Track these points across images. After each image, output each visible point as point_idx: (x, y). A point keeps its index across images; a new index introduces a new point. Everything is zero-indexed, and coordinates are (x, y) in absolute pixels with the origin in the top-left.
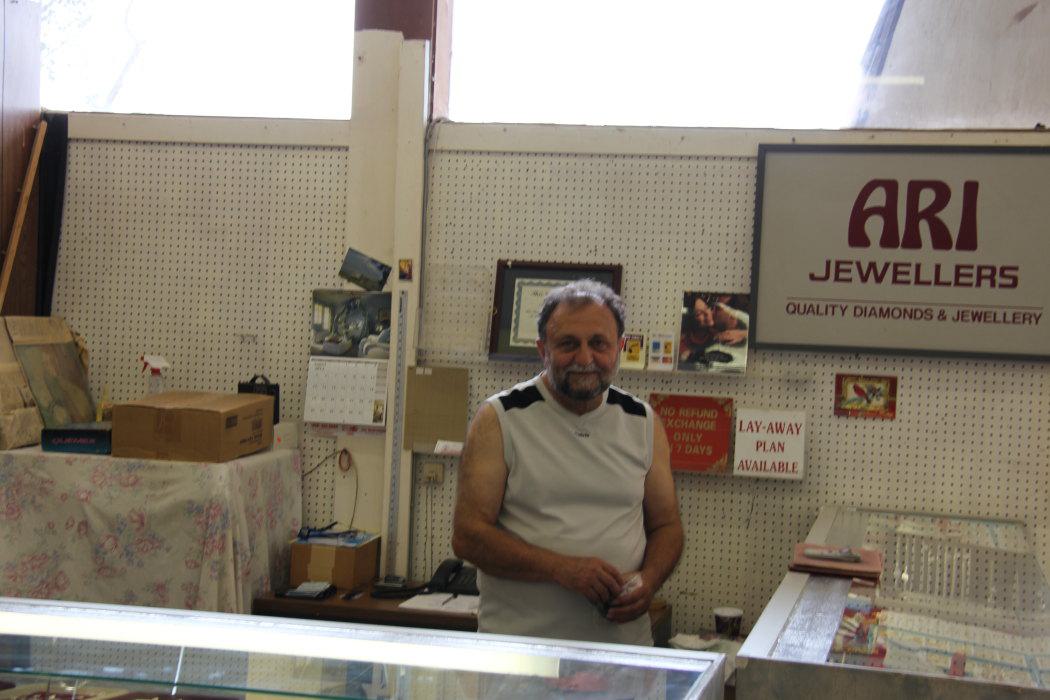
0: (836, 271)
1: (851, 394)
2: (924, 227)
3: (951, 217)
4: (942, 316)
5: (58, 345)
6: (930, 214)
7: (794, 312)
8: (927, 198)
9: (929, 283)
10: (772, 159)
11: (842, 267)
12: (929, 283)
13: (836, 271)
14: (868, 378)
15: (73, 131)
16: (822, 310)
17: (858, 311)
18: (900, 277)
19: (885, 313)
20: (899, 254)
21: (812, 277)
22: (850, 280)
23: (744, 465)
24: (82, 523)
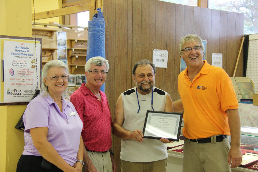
5: (247, 82)
15: (250, 39)
24: (248, 118)
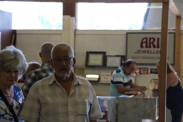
0: (139, 52)
2: (152, 45)
3: (156, 43)
4: (155, 58)
6: (152, 43)
8: (152, 40)
13: (139, 52)
19: (146, 58)
20: (148, 49)
21: (135, 53)
23: (102, 81)
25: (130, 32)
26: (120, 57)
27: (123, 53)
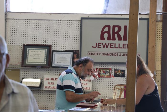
0: (98, 45)
1: (102, 72)
2: (116, 35)
3: (122, 33)
4: (120, 55)
6: (117, 33)
7: (89, 55)
8: (116, 29)
9: (117, 48)
10: (83, 21)
11: (99, 44)
12: (117, 48)
13: (98, 45)
14: (105, 69)
16: (95, 54)
17: (103, 54)
18: (111, 47)
19: (108, 55)
21: (93, 47)
22: (101, 47)
25: (86, 16)
26: (72, 53)
27: (76, 48)
